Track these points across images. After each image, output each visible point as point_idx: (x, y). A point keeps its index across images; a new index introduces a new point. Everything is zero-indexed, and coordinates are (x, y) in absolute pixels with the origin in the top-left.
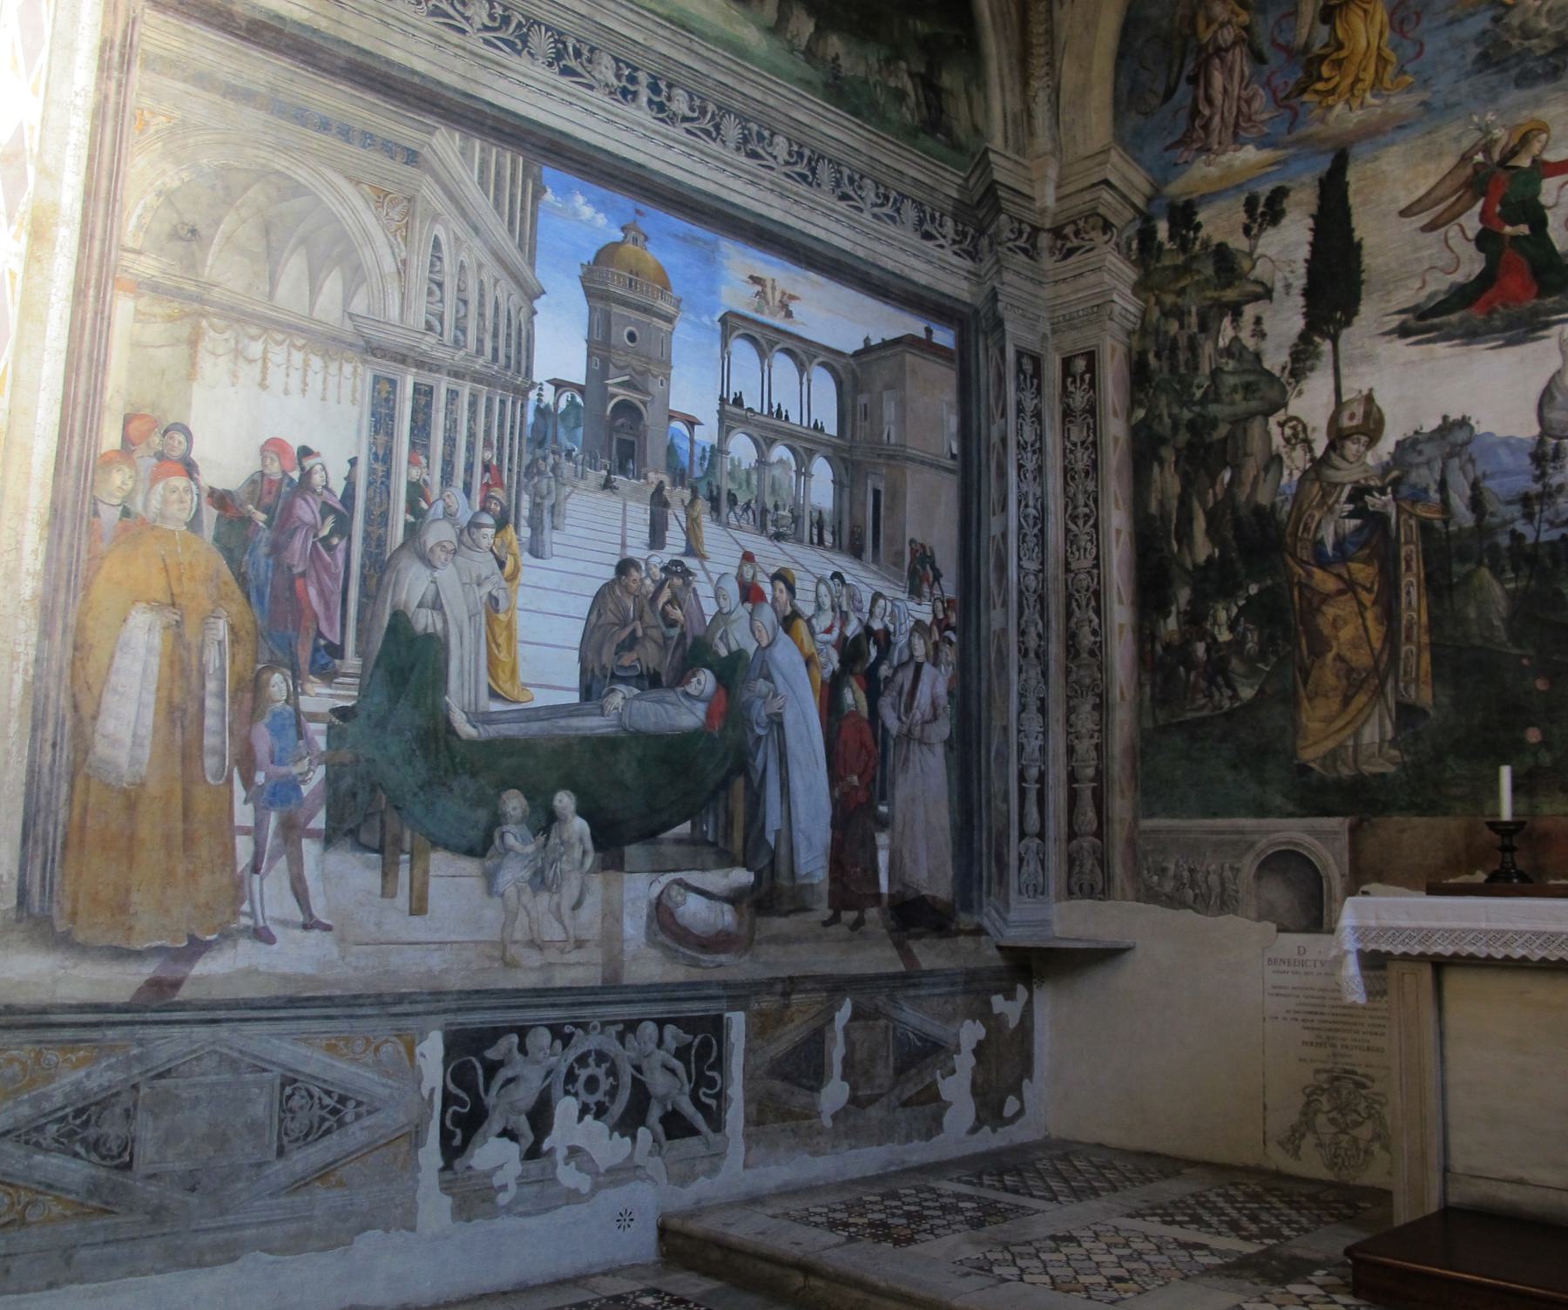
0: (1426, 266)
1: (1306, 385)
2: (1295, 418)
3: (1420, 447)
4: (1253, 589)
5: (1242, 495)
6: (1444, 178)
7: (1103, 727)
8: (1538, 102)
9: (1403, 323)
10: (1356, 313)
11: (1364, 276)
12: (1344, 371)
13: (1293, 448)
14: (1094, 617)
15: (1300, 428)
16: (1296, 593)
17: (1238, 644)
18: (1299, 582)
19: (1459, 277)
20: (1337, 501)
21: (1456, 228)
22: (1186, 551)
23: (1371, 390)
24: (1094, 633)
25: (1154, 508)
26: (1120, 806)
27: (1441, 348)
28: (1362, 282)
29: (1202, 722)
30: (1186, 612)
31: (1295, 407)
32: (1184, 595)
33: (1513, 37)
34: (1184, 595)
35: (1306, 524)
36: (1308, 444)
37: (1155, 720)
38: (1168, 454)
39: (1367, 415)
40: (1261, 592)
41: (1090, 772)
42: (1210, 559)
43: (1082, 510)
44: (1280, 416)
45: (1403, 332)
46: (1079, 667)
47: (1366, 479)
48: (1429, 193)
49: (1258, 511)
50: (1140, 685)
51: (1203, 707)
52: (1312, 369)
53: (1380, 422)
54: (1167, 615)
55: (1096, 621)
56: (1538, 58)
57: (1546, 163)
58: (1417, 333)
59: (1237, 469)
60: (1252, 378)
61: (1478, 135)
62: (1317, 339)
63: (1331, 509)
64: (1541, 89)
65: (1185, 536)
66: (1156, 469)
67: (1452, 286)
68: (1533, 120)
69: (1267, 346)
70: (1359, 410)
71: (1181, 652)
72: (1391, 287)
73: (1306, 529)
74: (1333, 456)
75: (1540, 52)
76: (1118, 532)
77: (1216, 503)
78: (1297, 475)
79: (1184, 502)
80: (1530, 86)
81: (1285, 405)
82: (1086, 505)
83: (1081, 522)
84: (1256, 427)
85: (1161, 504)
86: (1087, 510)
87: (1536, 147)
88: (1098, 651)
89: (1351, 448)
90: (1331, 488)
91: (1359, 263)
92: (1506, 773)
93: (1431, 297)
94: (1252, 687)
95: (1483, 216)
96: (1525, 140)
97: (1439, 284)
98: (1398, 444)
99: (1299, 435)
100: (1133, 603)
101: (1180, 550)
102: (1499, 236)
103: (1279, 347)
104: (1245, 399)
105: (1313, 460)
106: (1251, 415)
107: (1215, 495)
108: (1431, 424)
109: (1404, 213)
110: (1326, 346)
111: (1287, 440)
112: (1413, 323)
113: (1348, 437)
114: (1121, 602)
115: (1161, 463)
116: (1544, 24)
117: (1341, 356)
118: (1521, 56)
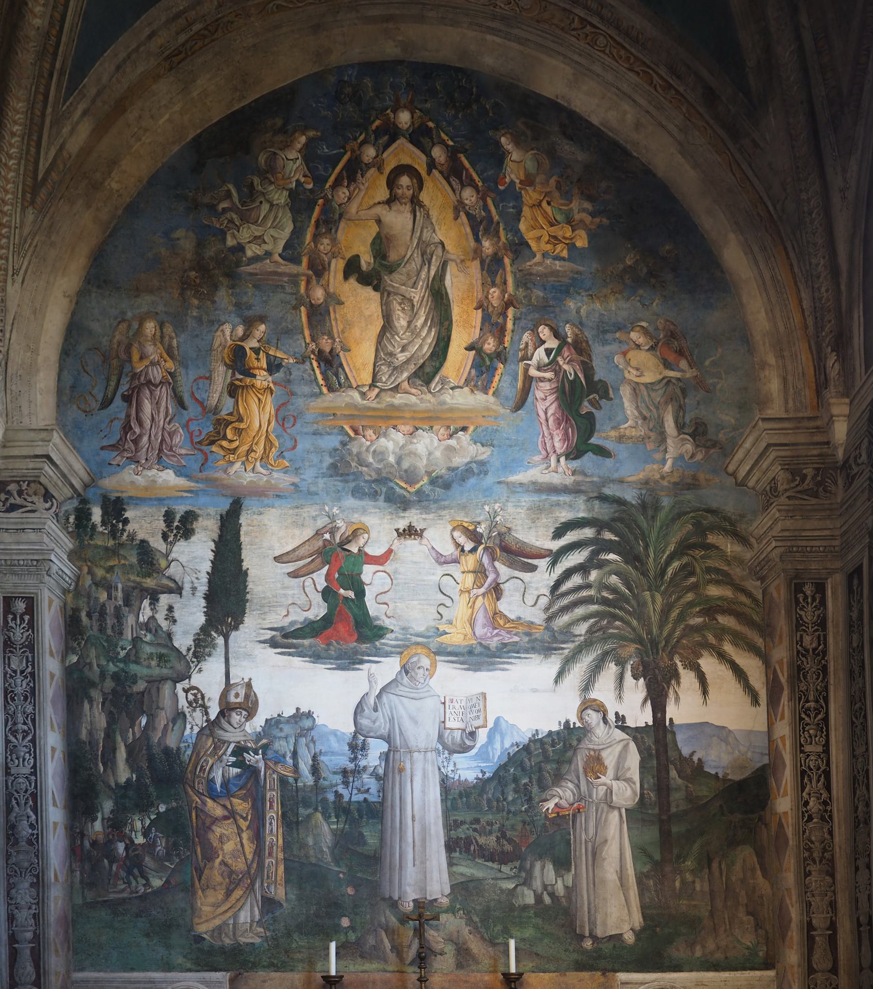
0: (290, 602)
1: (204, 665)
2: (196, 688)
3: (281, 726)
4: (162, 808)
5: (156, 737)
6: (304, 543)
7: (40, 900)
8: (364, 511)
9: (273, 637)
10: (242, 622)
11: (248, 597)
12: (232, 662)
13: (194, 710)
14: (31, 813)
15: (199, 696)
16: (194, 814)
17: (150, 846)
18: (196, 807)
19: (311, 615)
20: (224, 753)
21: (310, 580)
22: (109, 771)
23: (250, 679)
24: (32, 826)
25: (84, 735)
26: (55, 962)
27: (297, 661)
28: (247, 601)
29: (124, 900)
30: (109, 819)
31: (196, 680)
32: (108, 806)
33: (353, 460)
34: (108, 806)
35: (202, 766)
36: (205, 709)
37: (84, 897)
38: (96, 694)
39: (247, 696)
40: (167, 810)
41: (29, 935)
42: (129, 781)
43: (21, 727)
44: (185, 684)
45: (273, 643)
46: (18, 852)
47: (244, 741)
48: (294, 550)
49: (167, 751)
50: (72, 871)
51: (123, 891)
52: (210, 655)
53: (256, 703)
54: (94, 819)
55: (34, 817)
56: (366, 481)
57: (366, 554)
58: (282, 647)
59: (152, 718)
60: (164, 651)
61: (326, 520)
62: (213, 633)
63: (220, 759)
64: (367, 503)
65: (109, 758)
66: (86, 706)
67: (306, 619)
68: (360, 522)
69: (177, 629)
70: (242, 692)
71: (105, 848)
72: (267, 609)
73: (202, 769)
74: (223, 721)
75: (368, 478)
76: (53, 750)
77: (134, 740)
78: (196, 730)
79: (109, 735)
80: (361, 499)
81: (189, 677)
82: (25, 723)
83: (20, 737)
84: (167, 687)
85: (90, 733)
86: (25, 728)
87: (361, 542)
88: (36, 841)
89: (236, 718)
90: (220, 744)
91: (246, 587)
92: (333, 946)
93: (292, 623)
94: (161, 879)
95: (328, 577)
96: (355, 534)
97: (298, 617)
98: (267, 720)
99: (199, 701)
100: (65, 808)
101: (105, 770)
102: (336, 594)
103: (185, 633)
104: (158, 666)
105: (208, 721)
106: (163, 679)
107: (134, 733)
108: (289, 712)
109: (276, 559)
110: (220, 641)
111: (190, 703)
112: (279, 639)
113: (233, 709)
114: (55, 804)
115: (91, 701)
116: (371, 460)
117: (230, 650)
118: (358, 475)
